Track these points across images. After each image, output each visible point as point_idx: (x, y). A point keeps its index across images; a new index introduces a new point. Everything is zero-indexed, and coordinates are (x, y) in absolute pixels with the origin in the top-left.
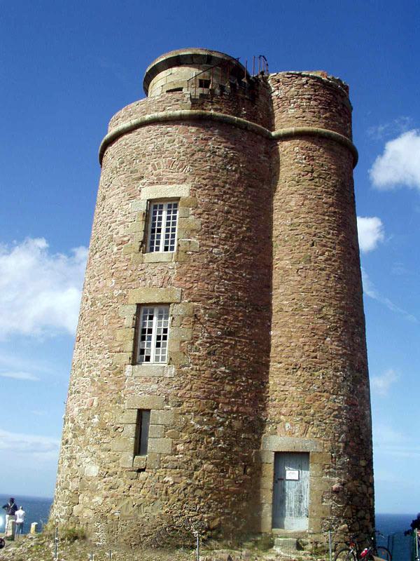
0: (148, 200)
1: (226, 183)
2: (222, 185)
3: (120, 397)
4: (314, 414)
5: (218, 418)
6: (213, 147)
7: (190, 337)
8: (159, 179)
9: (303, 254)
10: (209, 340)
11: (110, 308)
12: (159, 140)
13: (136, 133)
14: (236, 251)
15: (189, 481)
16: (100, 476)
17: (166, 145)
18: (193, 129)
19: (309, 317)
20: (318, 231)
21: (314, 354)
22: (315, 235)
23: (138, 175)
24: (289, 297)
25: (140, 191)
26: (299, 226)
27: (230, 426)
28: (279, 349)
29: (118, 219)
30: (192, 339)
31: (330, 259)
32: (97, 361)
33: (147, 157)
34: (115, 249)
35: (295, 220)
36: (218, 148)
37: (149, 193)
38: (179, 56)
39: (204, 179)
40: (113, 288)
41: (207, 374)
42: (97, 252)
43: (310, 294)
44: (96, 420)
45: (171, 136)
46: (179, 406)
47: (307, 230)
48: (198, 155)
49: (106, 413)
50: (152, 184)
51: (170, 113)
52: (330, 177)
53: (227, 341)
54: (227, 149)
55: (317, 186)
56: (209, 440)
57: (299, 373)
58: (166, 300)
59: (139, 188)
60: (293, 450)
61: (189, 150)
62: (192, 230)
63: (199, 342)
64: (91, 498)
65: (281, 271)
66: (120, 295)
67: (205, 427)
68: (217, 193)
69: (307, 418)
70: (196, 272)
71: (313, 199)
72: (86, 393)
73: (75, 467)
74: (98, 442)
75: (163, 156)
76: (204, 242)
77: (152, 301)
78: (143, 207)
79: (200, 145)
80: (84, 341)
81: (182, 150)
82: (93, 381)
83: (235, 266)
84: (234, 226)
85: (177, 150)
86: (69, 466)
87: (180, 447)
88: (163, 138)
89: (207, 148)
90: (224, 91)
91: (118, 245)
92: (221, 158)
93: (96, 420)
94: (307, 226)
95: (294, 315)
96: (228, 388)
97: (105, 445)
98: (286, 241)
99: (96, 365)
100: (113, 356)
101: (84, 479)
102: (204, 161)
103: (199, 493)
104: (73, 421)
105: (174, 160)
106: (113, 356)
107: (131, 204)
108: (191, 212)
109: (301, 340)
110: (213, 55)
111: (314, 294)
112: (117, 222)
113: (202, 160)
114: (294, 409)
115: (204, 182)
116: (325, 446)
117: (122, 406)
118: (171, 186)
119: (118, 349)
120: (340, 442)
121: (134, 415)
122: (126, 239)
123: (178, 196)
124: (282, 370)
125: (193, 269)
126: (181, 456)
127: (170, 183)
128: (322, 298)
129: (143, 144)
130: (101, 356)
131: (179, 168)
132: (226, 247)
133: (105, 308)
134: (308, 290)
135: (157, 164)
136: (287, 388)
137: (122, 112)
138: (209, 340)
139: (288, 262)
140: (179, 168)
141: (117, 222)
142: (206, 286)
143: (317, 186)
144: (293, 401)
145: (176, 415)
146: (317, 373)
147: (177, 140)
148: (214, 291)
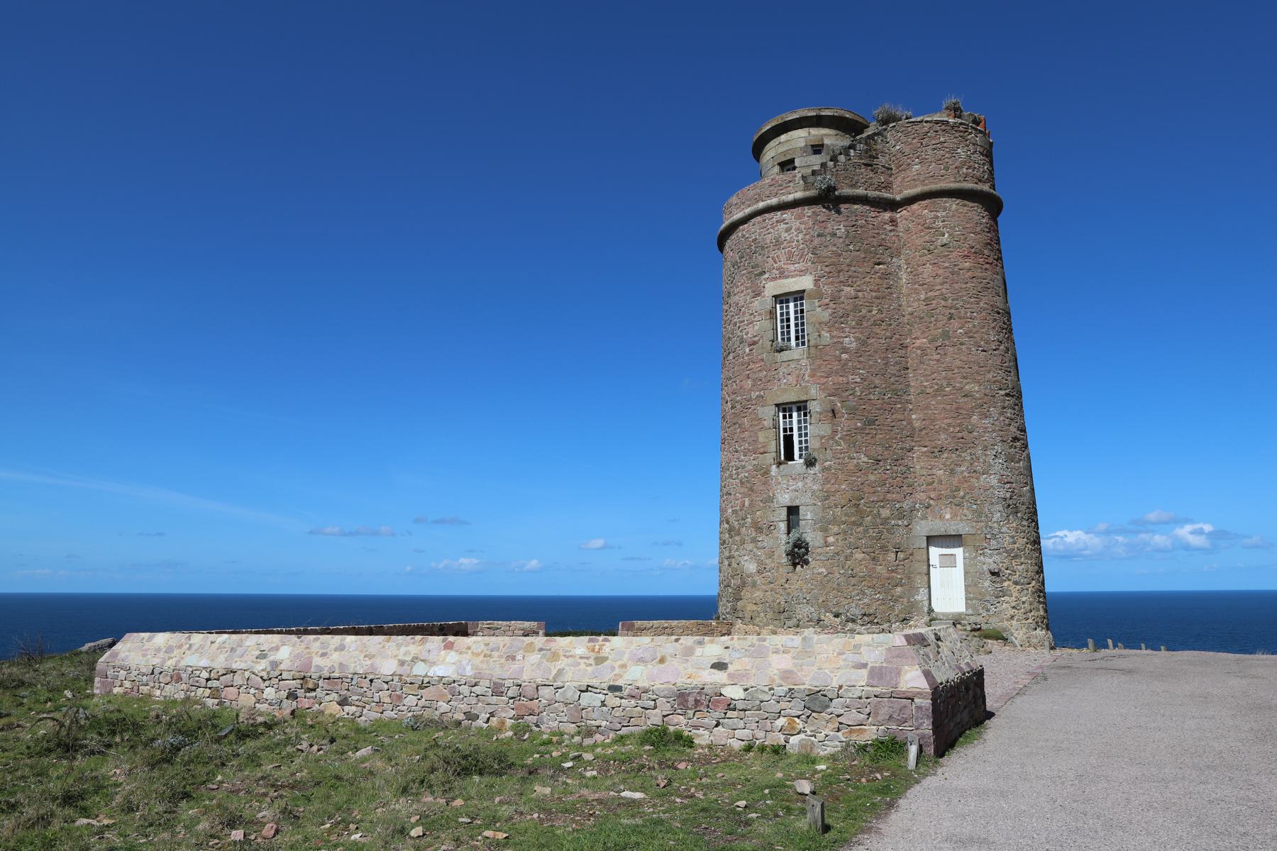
0: (773, 296)
1: (849, 265)
2: (847, 269)
3: (769, 496)
4: (964, 496)
5: (865, 508)
6: (833, 229)
7: (830, 432)
8: (782, 273)
9: (940, 330)
10: (849, 433)
11: (750, 410)
12: (776, 228)
13: (751, 224)
15: (842, 572)
16: (759, 572)
17: (784, 235)
19: (951, 397)
20: (955, 302)
21: (960, 435)
22: (951, 309)
23: (760, 270)
24: (929, 378)
25: (764, 287)
26: (934, 300)
27: (879, 514)
28: (923, 432)
29: (745, 319)
30: (832, 434)
31: (971, 331)
32: (744, 463)
33: (766, 250)
34: (747, 350)
35: (930, 294)
36: (839, 229)
37: (773, 288)
39: (827, 266)
40: (751, 390)
41: (851, 467)
42: (730, 353)
43: (951, 372)
44: (749, 520)
45: (787, 223)
46: (826, 499)
47: (943, 303)
48: (817, 241)
49: (758, 513)
50: (775, 279)
53: (867, 431)
55: (951, 252)
56: (858, 530)
57: (945, 455)
58: (804, 398)
59: (762, 285)
60: (945, 533)
61: (808, 237)
63: (839, 436)
64: (752, 593)
65: (919, 352)
66: (757, 396)
67: (853, 519)
68: (842, 280)
69: (956, 501)
70: (830, 366)
71: (947, 267)
72: (737, 495)
73: (734, 565)
74: (754, 541)
76: (835, 333)
77: (789, 401)
78: (769, 302)
79: (817, 229)
80: (729, 443)
81: (801, 236)
82: (742, 483)
83: (869, 353)
84: (864, 311)
85: (797, 238)
86: (729, 565)
87: (831, 539)
89: (827, 231)
90: (838, 161)
91: (749, 345)
92: (841, 240)
93: (749, 520)
94: (942, 299)
95: (935, 396)
96: (872, 478)
97: (759, 543)
98: (921, 318)
99: (744, 467)
100: (758, 457)
101: (744, 575)
103: (853, 581)
104: (728, 523)
105: (793, 250)
106: (758, 457)
107: (756, 302)
108: (817, 304)
109: (945, 421)
110: (823, 114)
111: (956, 371)
112: (746, 322)
114: (943, 492)
115: (827, 269)
116: (977, 527)
117: (772, 504)
118: (794, 279)
119: (762, 450)
120: (994, 522)
121: (784, 513)
122: (756, 339)
123: (803, 289)
124: (927, 454)
125: (825, 363)
126: (832, 548)
127: (793, 277)
128: (965, 375)
129: (760, 235)
130: (747, 458)
131: (800, 258)
132: (856, 335)
133: (745, 411)
135: (777, 256)
136: (934, 471)
137: (734, 199)
138: (849, 433)
139: (925, 340)
140: (800, 258)
141: (746, 322)
142: (841, 379)
143: (951, 252)
144: (941, 484)
145: (824, 509)
146: (963, 455)
147: (794, 228)
148: (847, 383)
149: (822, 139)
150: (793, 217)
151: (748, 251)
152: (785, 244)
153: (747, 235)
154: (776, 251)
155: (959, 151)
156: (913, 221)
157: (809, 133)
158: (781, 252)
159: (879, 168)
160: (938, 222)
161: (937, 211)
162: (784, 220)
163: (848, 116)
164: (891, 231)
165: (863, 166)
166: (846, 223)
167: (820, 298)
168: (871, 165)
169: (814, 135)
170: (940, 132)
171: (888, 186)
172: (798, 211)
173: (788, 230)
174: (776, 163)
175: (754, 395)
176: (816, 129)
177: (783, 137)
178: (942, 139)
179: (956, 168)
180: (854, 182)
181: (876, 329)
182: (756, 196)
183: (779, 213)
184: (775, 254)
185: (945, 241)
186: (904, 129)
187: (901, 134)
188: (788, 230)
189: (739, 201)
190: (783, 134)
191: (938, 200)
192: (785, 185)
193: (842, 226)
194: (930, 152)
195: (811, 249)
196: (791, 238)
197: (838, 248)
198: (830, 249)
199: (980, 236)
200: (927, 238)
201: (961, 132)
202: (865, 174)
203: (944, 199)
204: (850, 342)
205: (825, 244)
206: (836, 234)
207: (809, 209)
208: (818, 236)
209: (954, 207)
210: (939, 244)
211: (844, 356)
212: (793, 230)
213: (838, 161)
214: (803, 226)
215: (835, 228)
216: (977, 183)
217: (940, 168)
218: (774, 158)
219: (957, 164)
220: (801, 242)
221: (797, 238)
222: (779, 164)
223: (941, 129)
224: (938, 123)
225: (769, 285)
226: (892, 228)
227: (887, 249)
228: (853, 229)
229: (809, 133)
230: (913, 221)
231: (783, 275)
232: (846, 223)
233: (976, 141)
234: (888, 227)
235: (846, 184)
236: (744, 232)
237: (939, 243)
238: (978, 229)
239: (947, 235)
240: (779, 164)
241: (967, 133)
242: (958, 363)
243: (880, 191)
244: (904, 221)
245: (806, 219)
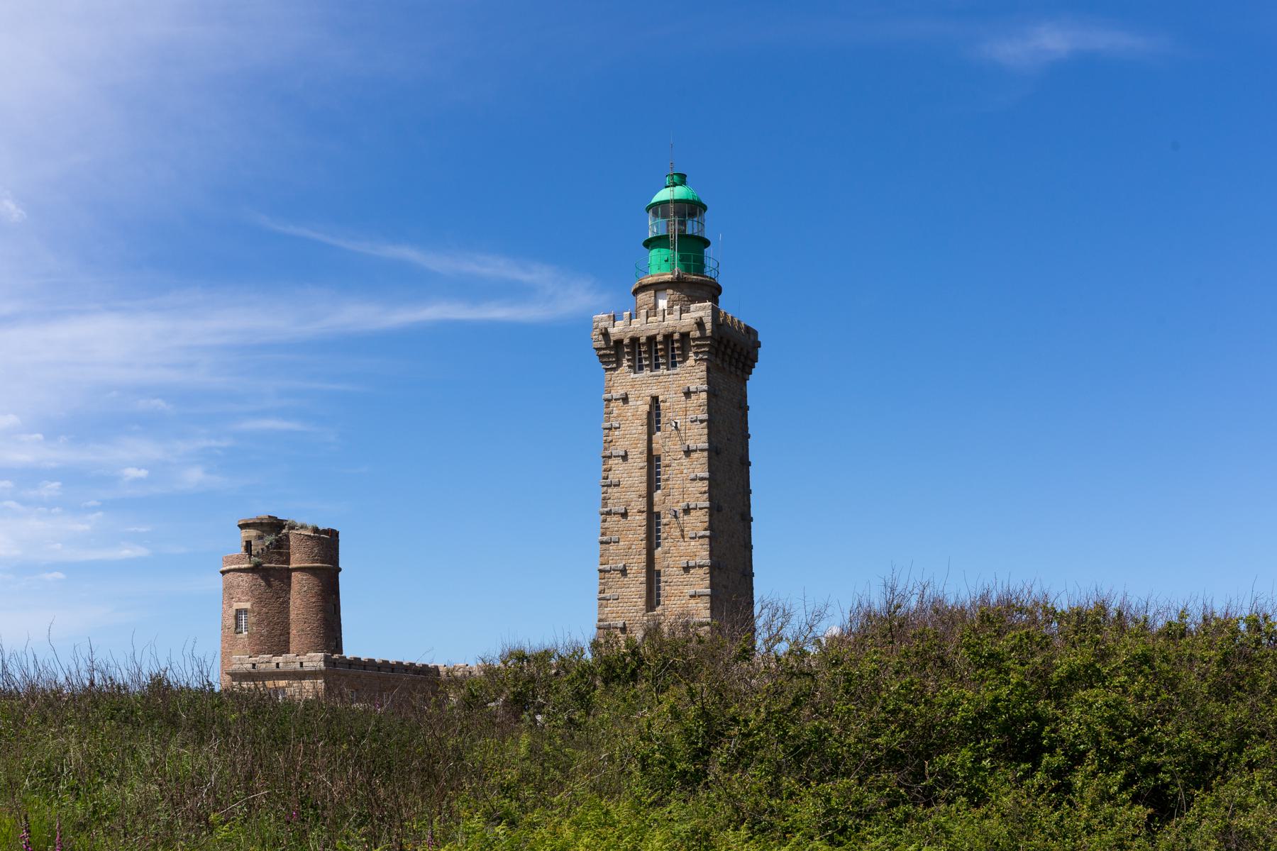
14: (273, 630)
18: (251, 575)
50: (237, 602)
51: (241, 566)
62: (253, 624)
79: (254, 582)
134: (303, 644)
167: (254, 613)
171: (287, 561)
175: (229, 651)
181: (276, 626)
204: (264, 632)
211: (262, 638)
225: (235, 604)
231: (239, 600)
242: (306, 642)
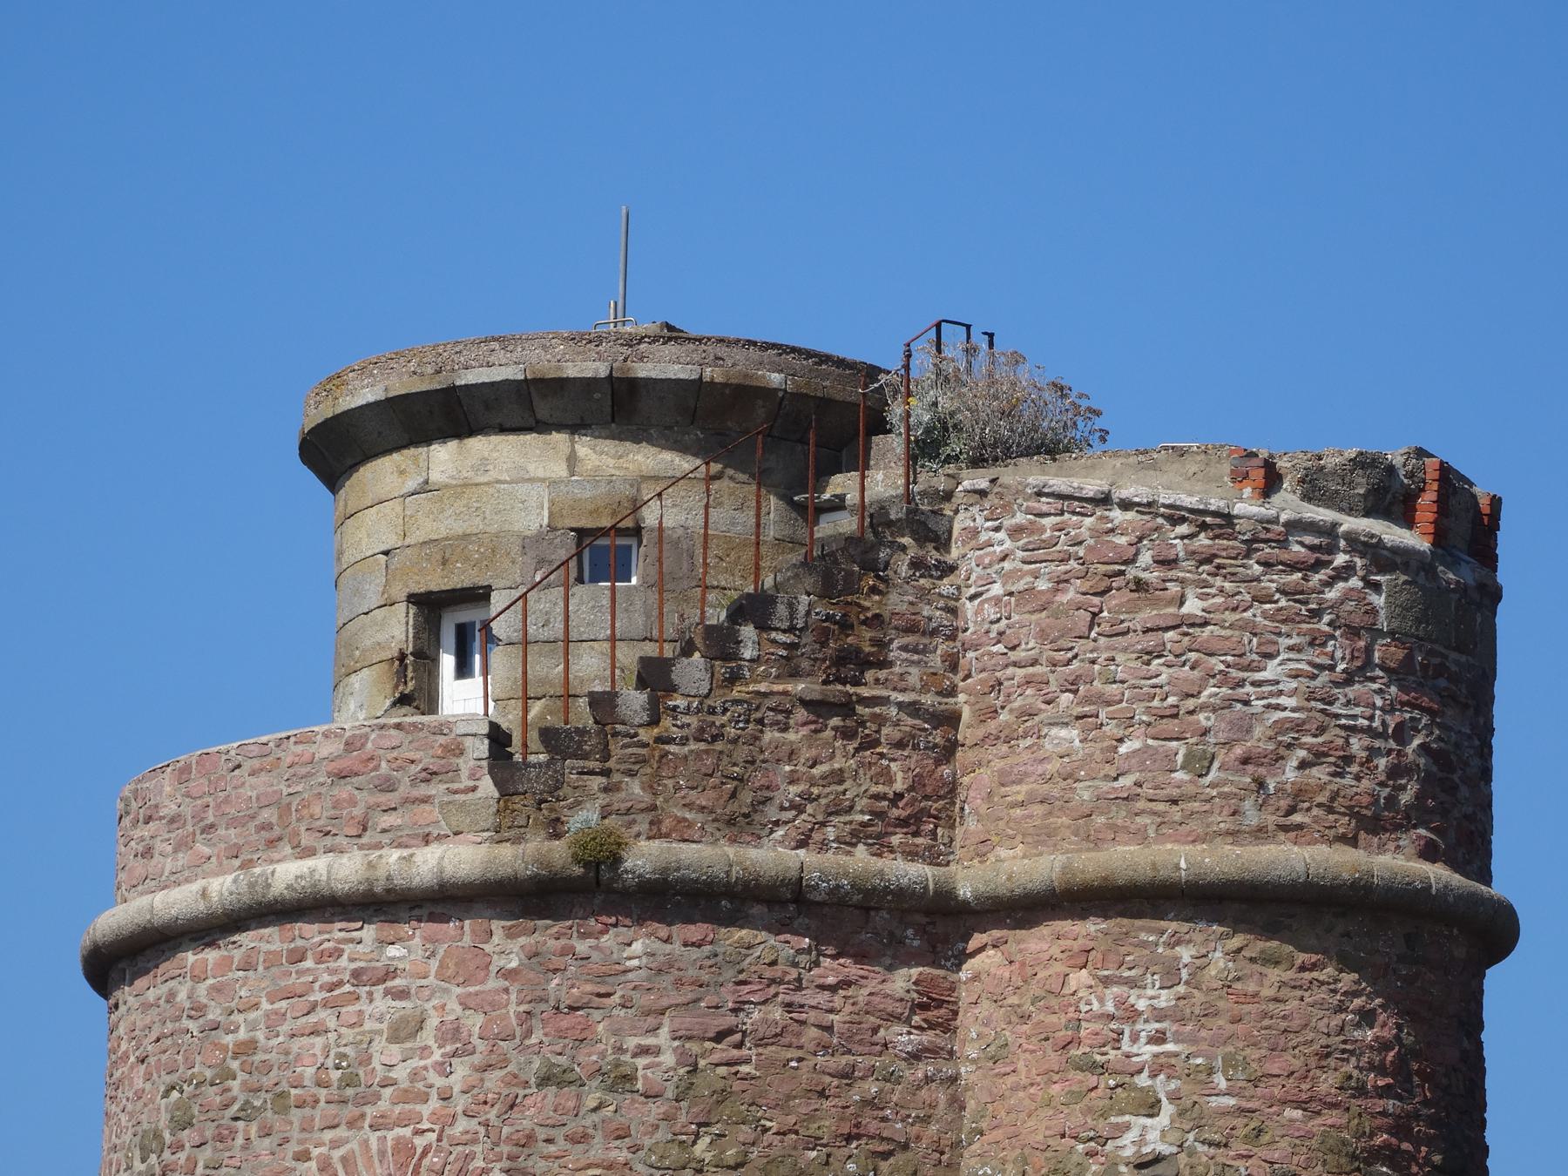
6: (620, 1050)
17: (385, 1053)
33: (296, 1115)
36: (644, 1051)
38: (452, 391)
45: (402, 994)
48: (538, 1106)
52: (1259, 1132)
54: (693, 1047)
61: (493, 1079)
75: (370, 1111)
81: (461, 1071)
85: (440, 1082)
88: (362, 1005)
89: (589, 1057)
90: (672, 689)
92: (656, 1109)
102: (574, 1140)
105: (419, 1142)
110: (643, 371)
113: (558, 1134)
129: (272, 1032)
147: (433, 1022)
149: (637, 506)
150: (434, 964)
151: (212, 1095)
152: (383, 1105)
153: (214, 1014)
154: (342, 1132)
155: (1272, 670)
156: (1025, 1018)
157: (572, 460)
158: (365, 1144)
159: (881, 720)
160: (1135, 1038)
161: (1132, 983)
162: (390, 974)
163: (776, 379)
164: (915, 1057)
165: (801, 714)
166: (687, 1021)
168: (846, 708)
169: (594, 478)
170: (1185, 570)
172: (460, 933)
173: (405, 1030)
174: (400, 591)
176: (609, 445)
177: (443, 459)
178: (1193, 606)
179: (1245, 761)
180: (747, 797)
182: (266, 815)
183: (369, 932)
184: (335, 1144)
185: (1155, 1144)
186: (1020, 518)
187: (1008, 544)
188: (405, 1030)
189: (187, 811)
190: (444, 435)
191: (1147, 932)
192: (404, 789)
193: (663, 1038)
194: (1126, 665)
195: (505, 1149)
196: (415, 1075)
197: (635, 1149)
198: (597, 1151)
199: (1332, 1117)
200: (1075, 1119)
201: (1293, 567)
202: (806, 754)
203: (1172, 926)
205: (573, 1127)
206: (629, 1078)
207: (510, 934)
208: (544, 1081)
209: (1219, 961)
210: (1129, 1152)
212: (428, 1037)
213: (672, 689)
214: (475, 1022)
215: (632, 1042)
216: (1353, 841)
217: (1171, 756)
218: (396, 561)
219: (1258, 740)
220: (461, 1103)
221: (440, 1082)
222: (414, 599)
223: (1191, 554)
224: (1183, 520)
226: (927, 1038)
227: (886, 1155)
228: (724, 1051)
229: (572, 460)
230: (1025, 1018)
232: (687, 1021)
233: (1373, 611)
234: (904, 1038)
235: (702, 809)
236: (202, 989)
237: (1127, 1146)
238: (1327, 1083)
239: (1167, 1109)
240: (413, 599)
241: (1322, 575)
243: (880, 846)
244: (986, 1007)
245: (493, 983)
